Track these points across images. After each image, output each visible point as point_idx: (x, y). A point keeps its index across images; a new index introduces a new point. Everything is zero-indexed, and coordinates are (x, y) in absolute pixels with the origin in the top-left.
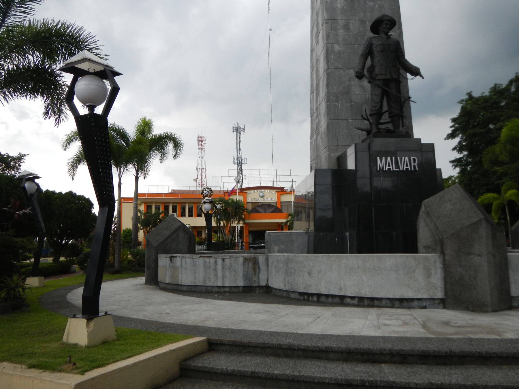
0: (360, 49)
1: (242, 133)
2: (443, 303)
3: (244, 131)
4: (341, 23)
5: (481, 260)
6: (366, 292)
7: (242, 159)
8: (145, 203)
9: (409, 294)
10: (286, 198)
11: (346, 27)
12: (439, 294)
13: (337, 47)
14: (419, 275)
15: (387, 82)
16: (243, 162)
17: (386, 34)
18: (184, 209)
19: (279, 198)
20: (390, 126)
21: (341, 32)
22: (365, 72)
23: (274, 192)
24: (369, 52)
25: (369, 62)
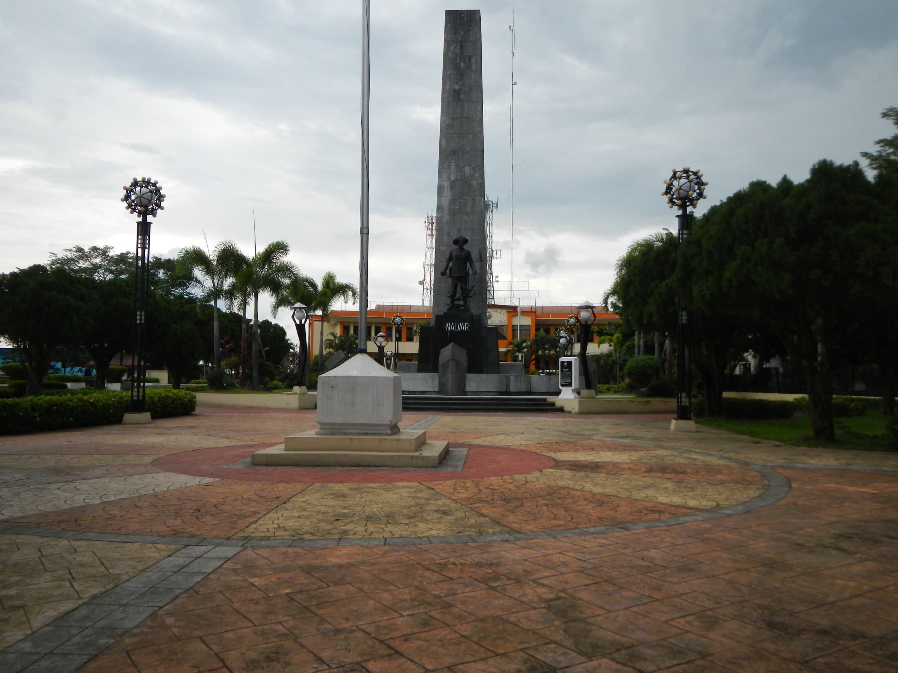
0: (448, 255)
1: (494, 210)
2: (438, 393)
3: (497, 207)
4: (446, 231)
5: (450, 376)
6: (411, 389)
7: (493, 251)
8: (341, 323)
9: (426, 390)
10: (517, 321)
11: (449, 234)
12: (437, 390)
13: (442, 248)
14: (430, 381)
15: (459, 279)
16: (495, 255)
17: (462, 249)
18: (389, 329)
19: (510, 320)
20: (462, 303)
21: (445, 237)
22: (448, 271)
23: (504, 311)
24: (450, 259)
25: (451, 264)
